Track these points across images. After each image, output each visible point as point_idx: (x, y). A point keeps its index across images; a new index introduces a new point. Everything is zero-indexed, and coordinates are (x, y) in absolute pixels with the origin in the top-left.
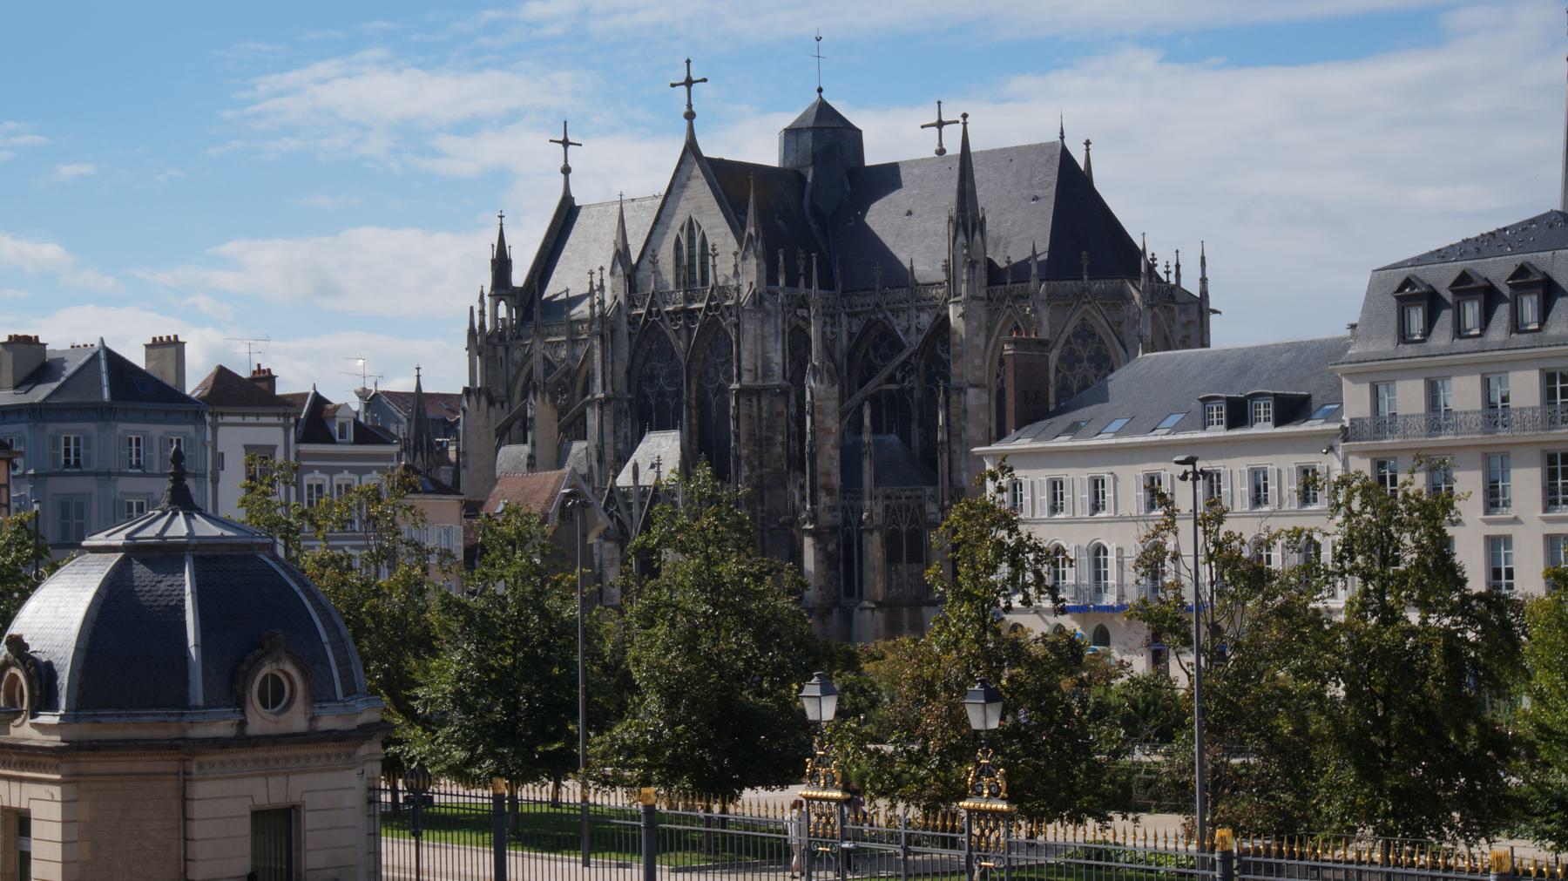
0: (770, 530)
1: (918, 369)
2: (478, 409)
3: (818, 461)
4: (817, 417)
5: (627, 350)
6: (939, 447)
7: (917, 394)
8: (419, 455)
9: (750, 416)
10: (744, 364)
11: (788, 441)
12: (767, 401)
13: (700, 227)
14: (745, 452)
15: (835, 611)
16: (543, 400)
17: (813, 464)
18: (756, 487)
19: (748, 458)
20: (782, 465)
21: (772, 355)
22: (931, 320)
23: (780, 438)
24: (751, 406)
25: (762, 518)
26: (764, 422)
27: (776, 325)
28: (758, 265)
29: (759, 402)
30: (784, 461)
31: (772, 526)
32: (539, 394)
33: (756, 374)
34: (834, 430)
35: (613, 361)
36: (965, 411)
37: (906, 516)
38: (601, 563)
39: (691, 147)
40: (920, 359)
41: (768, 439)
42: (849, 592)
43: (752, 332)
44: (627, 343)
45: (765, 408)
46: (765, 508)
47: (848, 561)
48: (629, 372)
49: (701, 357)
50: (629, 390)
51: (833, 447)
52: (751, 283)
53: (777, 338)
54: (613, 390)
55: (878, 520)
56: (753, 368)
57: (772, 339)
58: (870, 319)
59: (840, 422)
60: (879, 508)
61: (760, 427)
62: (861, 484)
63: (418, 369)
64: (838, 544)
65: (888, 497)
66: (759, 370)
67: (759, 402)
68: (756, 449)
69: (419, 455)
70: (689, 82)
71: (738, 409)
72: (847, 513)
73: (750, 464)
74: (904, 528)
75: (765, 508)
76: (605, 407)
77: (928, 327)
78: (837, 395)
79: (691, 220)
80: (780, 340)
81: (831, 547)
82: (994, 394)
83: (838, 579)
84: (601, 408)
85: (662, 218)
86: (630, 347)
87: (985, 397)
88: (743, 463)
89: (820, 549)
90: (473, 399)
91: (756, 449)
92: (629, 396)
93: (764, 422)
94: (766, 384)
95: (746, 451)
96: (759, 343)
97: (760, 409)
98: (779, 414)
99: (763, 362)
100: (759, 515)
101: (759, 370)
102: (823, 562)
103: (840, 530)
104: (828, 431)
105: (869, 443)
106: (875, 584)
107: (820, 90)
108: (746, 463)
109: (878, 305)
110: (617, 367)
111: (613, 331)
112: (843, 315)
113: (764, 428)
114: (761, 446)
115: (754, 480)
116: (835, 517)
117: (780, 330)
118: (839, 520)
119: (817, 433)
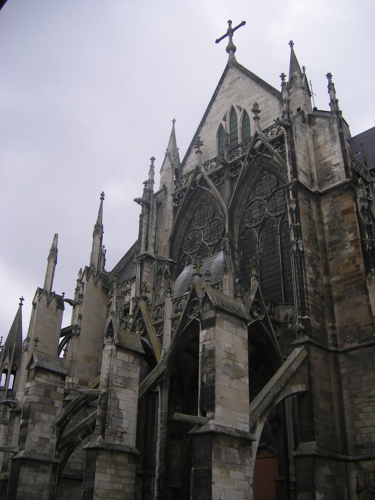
0: (346, 352)
5: (171, 222)
8: (8, 357)
9: (310, 218)
11: (362, 235)
16: (96, 284)
20: (358, 266)
23: (351, 237)
25: (334, 336)
26: (326, 228)
27: (332, 131)
30: (360, 261)
31: (348, 346)
32: (91, 277)
35: (157, 228)
38: (108, 381)
39: (233, 64)
41: (331, 244)
44: (171, 216)
45: (325, 213)
48: (172, 239)
49: (244, 202)
50: (171, 256)
54: (155, 252)
57: (329, 144)
61: (323, 231)
63: (22, 299)
66: (315, 177)
67: (319, 206)
69: (8, 357)
70: (230, 32)
71: (297, 202)
76: (145, 264)
79: (233, 109)
80: (338, 139)
84: (142, 266)
85: (207, 120)
86: (174, 220)
88: (307, 262)
90: (44, 298)
93: (326, 228)
94: (324, 189)
98: (344, 213)
100: (330, 332)
110: (161, 236)
111: (159, 205)
114: (325, 251)
117: (337, 134)
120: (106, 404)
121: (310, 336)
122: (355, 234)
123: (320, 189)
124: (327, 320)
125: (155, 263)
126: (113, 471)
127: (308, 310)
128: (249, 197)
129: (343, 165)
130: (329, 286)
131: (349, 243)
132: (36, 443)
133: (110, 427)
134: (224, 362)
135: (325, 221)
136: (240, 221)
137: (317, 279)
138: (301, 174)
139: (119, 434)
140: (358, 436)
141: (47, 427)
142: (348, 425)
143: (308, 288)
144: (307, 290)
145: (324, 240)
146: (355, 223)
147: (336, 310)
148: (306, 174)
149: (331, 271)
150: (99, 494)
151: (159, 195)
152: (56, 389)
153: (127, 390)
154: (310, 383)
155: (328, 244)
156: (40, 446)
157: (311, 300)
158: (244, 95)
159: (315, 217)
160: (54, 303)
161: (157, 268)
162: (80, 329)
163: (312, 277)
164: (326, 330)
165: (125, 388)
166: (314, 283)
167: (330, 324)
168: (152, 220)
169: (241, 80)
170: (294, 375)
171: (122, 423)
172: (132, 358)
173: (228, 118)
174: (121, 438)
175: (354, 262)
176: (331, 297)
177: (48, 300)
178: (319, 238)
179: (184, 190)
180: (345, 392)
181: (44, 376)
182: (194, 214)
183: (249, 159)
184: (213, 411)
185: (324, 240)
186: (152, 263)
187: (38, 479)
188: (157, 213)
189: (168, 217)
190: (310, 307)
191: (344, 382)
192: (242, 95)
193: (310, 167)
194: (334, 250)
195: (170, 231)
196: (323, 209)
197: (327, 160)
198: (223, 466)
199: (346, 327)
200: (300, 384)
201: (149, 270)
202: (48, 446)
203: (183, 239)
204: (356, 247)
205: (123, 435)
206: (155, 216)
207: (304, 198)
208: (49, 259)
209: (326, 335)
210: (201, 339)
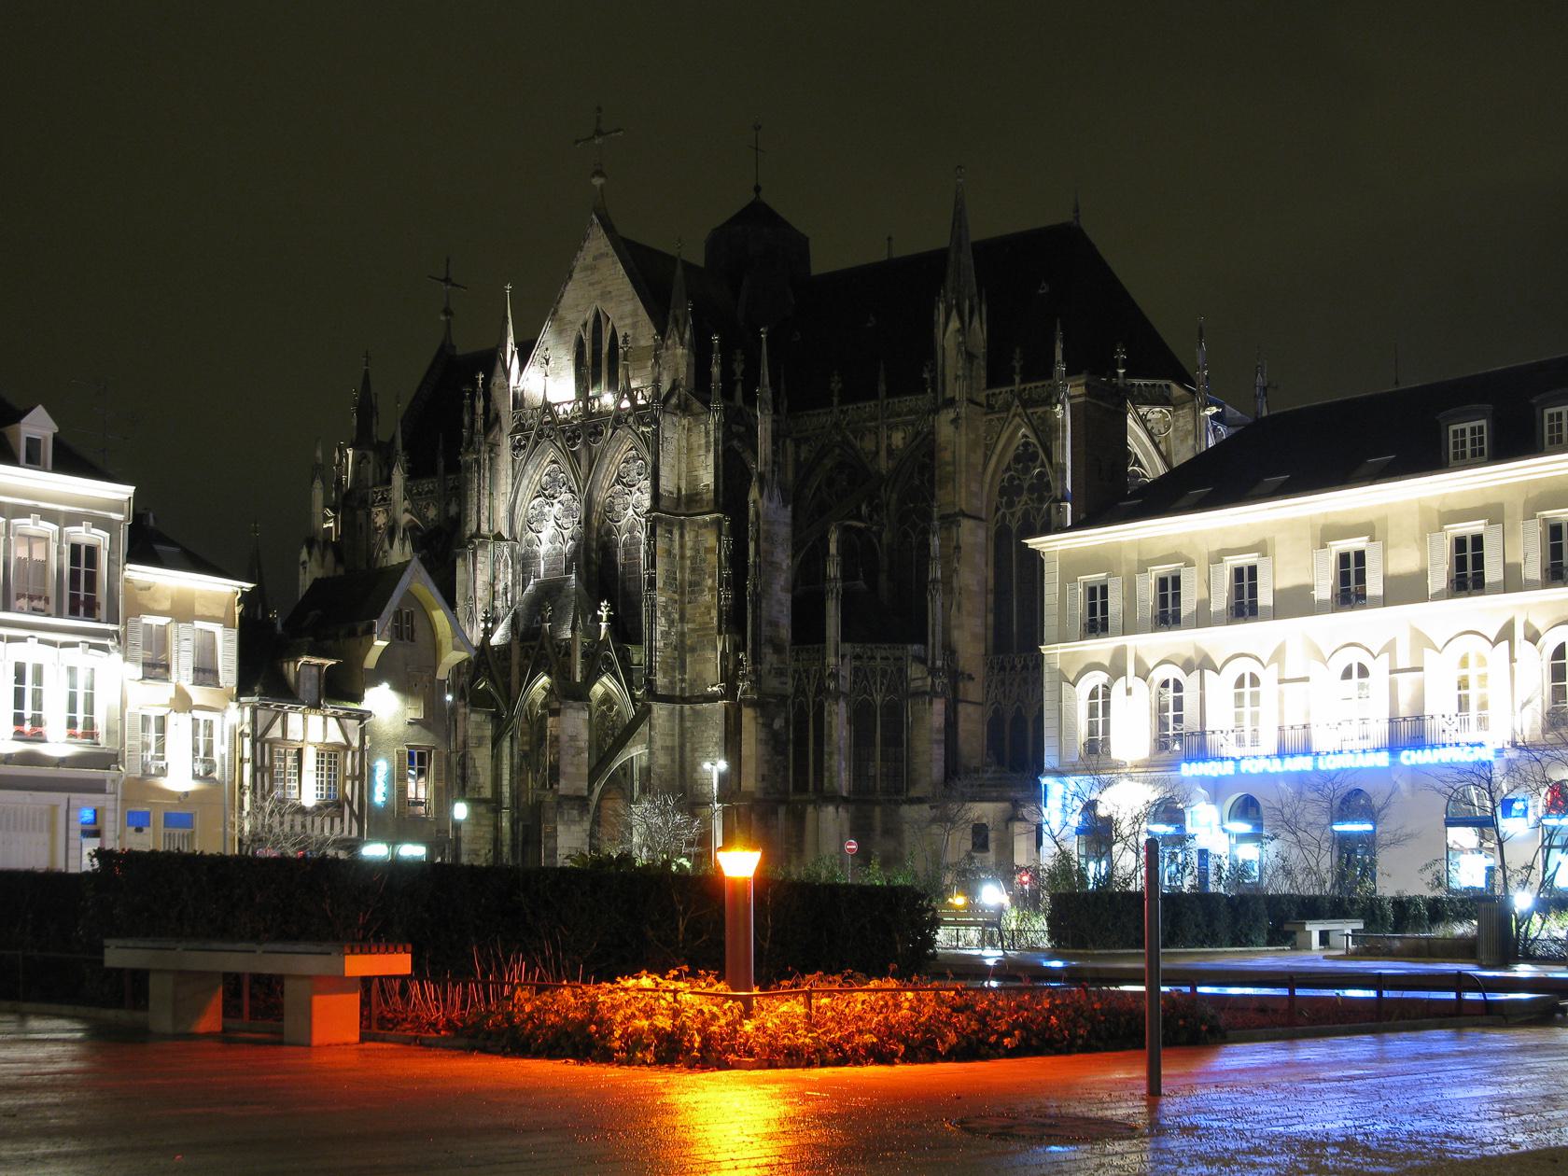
1: (888, 504)
3: (764, 605)
4: (763, 545)
6: (930, 587)
7: (886, 537)
12: (692, 534)
13: (608, 319)
14: (661, 599)
17: (756, 607)
18: (675, 648)
19: (665, 607)
20: (712, 619)
21: (701, 472)
26: (688, 562)
27: (707, 433)
29: (682, 536)
30: (714, 613)
34: (785, 567)
36: (958, 548)
37: (882, 684)
40: (891, 492)
42: (801, 787)
43: (675, 442)
45: (689, 544)
46: (687, 677)
47: (801, 743)
51: (783, 589)
53: (708, 451)
55: (845, 686)
57: (702, 452)
59: (793, 557)
60: (845, 672)
61: (682, 569)
62: (822, 638)
65: (858, 657)
67: (682, 536)
68: (677, 597)
72: (800, 679)
73: (668, 615)
74: (878, 699)
75: (687, 677)
77: (901, 446)
78: (789, 520)
80: (712, 449)
81: (778, 724)
82: (992, 533)
83: (786, 768)
87: (982, 534)
88: (659, 614)
91: (677, 597)
95: (664, 599)
97: (682, 547)
98: (708, 550)
99: (688, 483)
103: (790, 701)
105: (835, 578)
106: (840, 774)
107: (757, 189)
109: (836, 425)
112: (788, 441)
113: (688, 571)
114: (682, 593)
115: (674, 639)
116: (786, 684)
118: (790, 689)
120: (464, 764)
122: (714, 581)
123: (688, 510)
124: (677, 672)
130: (682, 634)
131: (706, 589)
134: (567, 745)
135: (688, 553)
145: (683, 580)
146: (715, 568)
149: (687, 616)
158: (613, 294)
159: (676, 550)
165: (478, 747)
166: (666, 634)
167: (678, 677)
168: (483, 482)
173: (590, 326)
174: (479, 791)
175: (710, 614)
176: (683, 648)
184: (558, 784)
185: (683, 580)
188: (490, 469)
189: (503, 473)
191: (689, 736)
194: (693, 592)
196: (687, 538)
197: (696, 473)
198: (565, 823)
199: (695, 681)
201: (483, 559)
206: (487, 475)
210: (549, 725)
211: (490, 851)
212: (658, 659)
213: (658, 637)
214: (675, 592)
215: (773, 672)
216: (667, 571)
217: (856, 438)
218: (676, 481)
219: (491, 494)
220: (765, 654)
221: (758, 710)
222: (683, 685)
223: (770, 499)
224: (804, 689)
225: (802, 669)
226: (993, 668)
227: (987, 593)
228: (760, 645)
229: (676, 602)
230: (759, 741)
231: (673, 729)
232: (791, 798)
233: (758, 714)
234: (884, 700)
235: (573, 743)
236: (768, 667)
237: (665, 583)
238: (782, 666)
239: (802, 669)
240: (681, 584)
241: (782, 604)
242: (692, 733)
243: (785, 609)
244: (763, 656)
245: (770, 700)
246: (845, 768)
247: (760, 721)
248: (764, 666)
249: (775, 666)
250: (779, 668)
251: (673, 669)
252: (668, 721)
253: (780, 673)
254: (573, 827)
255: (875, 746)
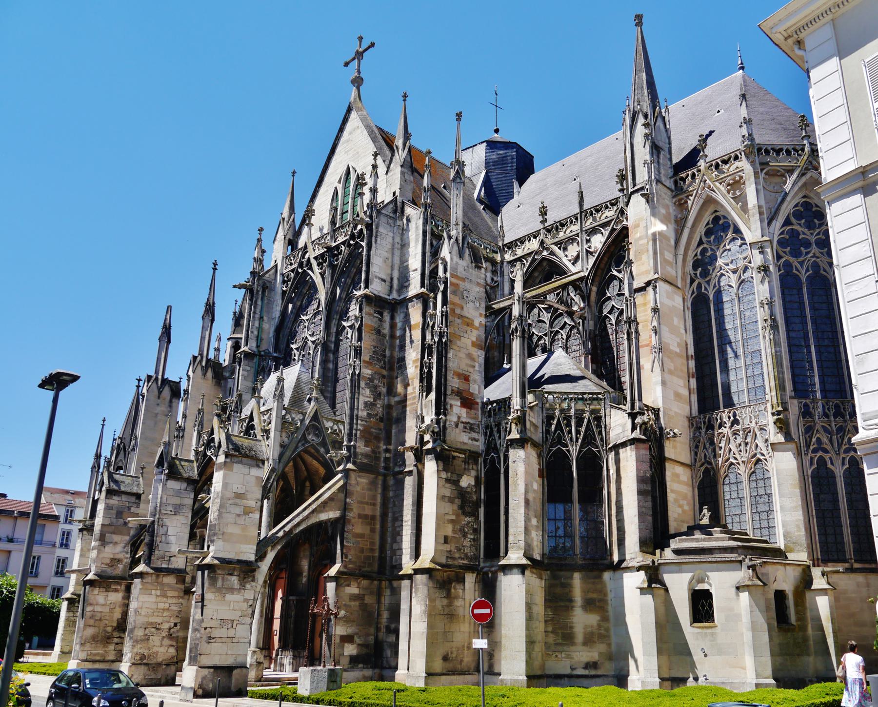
2: (159, 398)
3: (450, 355)
9: (379, 332)
10: (374, 269)
15: (470, 579)
16: (205, 374)
18: (381, 420)
19: (371, 380)
22: (603, 240)
24: (381, 320)
25: (387, 460)
26: (398, 341)
28: (402, 173)
29: (392, 318)
33: (391, 287)
34: (477, 323)
35: (261, 318)
37: (578, 432)
52: (394, 194)
56: (388, 279)
58: (534, 260)
64: (477, 479)
66: (395, 282)
67: (392, 318)
68: (385, 373)
72: (491, 434)
77: (599, 246)
81: (466, 481)
83: (476, 531)
88: (363, 384)
89: (447, 480)
91: (385, 373)
92: (275, 355)
95: (369, 372)
96: (397, 253)
100: (383, 455)
101: (395, 282)
102: (451, 500)
103: (481, 460)
104: (469, 323)
108: (366, 384)
110: (266, 326)
113: (397, 349)
114: (391, 369)
115: (379, 409)
116: (477, 440)
118: (480, 445)
119: (450, 318)
121: (354, 463)
123: (399, 296)
125: (256, 360)
126: (158, 593)
127: (356, 435)
128: (349, 290)
129: (419, 272)
132: (107, 564)
133: (157, 552)
136: (338, 317)
137: (375, 400)
138: (375, 283)
139: (167, 559)
140: (394, 557)
141: (119, 548)
142: (388, 546)
143: (360, 413)
144: (357, 416)
145: (392, 356)
147: (393, 431)
148: (384, 281)
150: (143, 613)
151: (267, 275)
152: (129, 509)
153: (177, 517)
154: (345, 508)
155: (396, 360)
156: (112, 566)
157: (360, 424)
160: (167, 392)
161: (259, 365)
162: (184, 430)
163: (367, 399)
164: (379, 453)
166: (368, 405)
167: (384, 447)
168: (255, 308)
169: (359, 131)
170: (325, 503)
171: (170, 548)
172: (185, 485)
174: (169, 561)
177: (159, 389)
178: (388, 353)
179: (292, 271)
180: (390, 515)
181: (114, 497)
182: (302, 301)
183: (349, 245)
185: (392, 356)
186: (253, 359)
187: (109, 598)
189: (275, 303)
190: (358, 432)
191: (391, 505)
192: (358, 153)
193: (392, 269)
195: (277, 320)
200: (331, 510)
201: (248, 368)
202: (121, 566)
203: (291, 330)
204: (416, 367)
205: (172, 559)
207: (372, 312)
208: (160, 339)
209: (377, 459)
211: (175, 625)
212: (359, 427)
213: (361, 406)
214: (384, 368)
215: (461, 426)
216: (375, 347)
217: (560, 248)
218: (389, 272)
219: (261, 318)
220: (451, 406)
221: (441, 463)
222: (388, 455)
223: (461, 256)
224: (496, 445)
225: (493, 424)
226: (700, 428)
227: (688, 359)
228: (445, 395)
229: (384, 377)
230: (441, 498)
231: (374, 497)
232: (482, 565)
233: (441, 468)
234: (580, 451)
235: (238, 501)
236: (455, 419)
237: (371, 358)
238: (472, 421)
239: (493, 424)
240: (389, 361)
241: (473, 360)
242: (394, 502)
243: (477, 364)
244: (448, 407)
245: (456, 454)
246: (537, 527)
247: (444, 475)
248: (448, 417)
249: (464, 420)
250: (468, 423)
251: (377, 438)
252: (370, 490)
253: (470, 428)
254: (229, 597)
255: (571, 502)
